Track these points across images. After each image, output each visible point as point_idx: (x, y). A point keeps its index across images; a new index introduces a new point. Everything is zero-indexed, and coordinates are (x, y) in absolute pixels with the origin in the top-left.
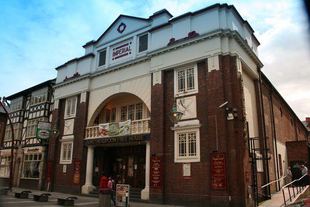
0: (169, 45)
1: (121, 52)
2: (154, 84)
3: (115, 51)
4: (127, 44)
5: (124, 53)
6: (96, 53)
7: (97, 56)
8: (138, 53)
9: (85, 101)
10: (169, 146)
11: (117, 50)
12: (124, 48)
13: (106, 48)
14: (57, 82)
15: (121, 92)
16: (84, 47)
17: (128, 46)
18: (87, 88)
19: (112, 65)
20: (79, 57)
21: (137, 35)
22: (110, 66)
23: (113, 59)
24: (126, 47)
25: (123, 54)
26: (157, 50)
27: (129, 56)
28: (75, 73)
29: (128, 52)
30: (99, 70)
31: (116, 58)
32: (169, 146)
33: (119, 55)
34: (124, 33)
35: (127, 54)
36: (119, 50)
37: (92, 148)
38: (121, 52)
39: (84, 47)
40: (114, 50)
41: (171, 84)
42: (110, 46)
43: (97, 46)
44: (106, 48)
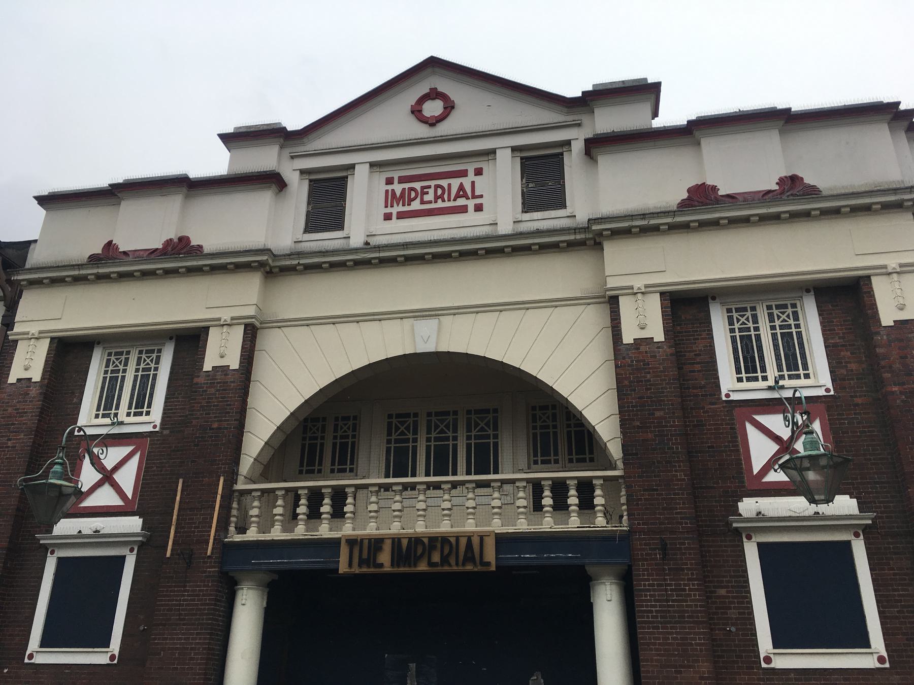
0: (685, 205)
1: (430, 197)
2: (628, 338)
3: (398, 188)
4: (464, 173)
5: (447, 204)
6: (290, 172)
7: (299, 190)
8: (300, 236)
9: (234, 363)
10: (723, 592)
11: (407, 186)
12: (444, 183)
13: (352, 167)
14: (36, 257)
15: (443, 348)
16: (226, 138)
17: (466, 182)
18: (251, 311)
19: (383, 240)
20: (195, 173)
21: (514, 149)
22: (374, 241)
23: (388, 217)
24: (455, 183)
25: (440, 204)
26: (643, 216)
27: (471, 217)
28: (172, 234)
29: (471, 204)
30: (523, 227)
31: (401, 216)
32: (723, 592)
33: (416, 205)
34: (443, 129)
35: (463, 209)
36: (417, 185)
37: (260, 585)
38: (426, 198)
39: (226, 138)
40: (389, 181)
41: (700, 346)
42: (372, 165)
43: (301, 149)
44: (352, 167)
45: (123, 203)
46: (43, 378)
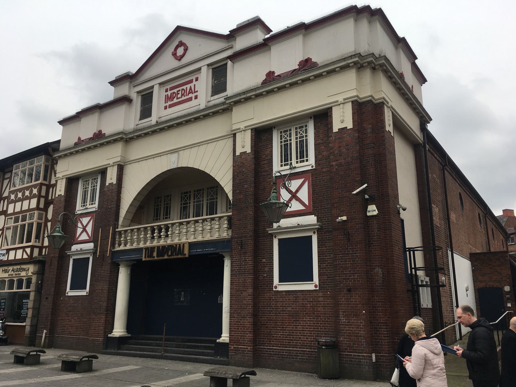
2: (238, 154)
3: (169, 93)
4: (191, 81)
7: (137, 101)
9: (114, 181)
10: (264, 260)
12: (184, 87)
13: (152, 87)
14: (62, 146)
15: (180, 166)
16: (112, 83)
17: (192, 85)
18: (119, 159)
19: (164, 119)
20: (102, 101)
21: (208, 65)
23: (166, 108)
24: (188, 86)
25: (183, 98)
26: (244, 93)
27: (194, 102)
30: (140, 126)
31: (171, 106)
32: (264, 260)
33: (175, 100)
34: (185, 60)
35: (190, 99)
36: (175, 91)
37: (127, 266)
38: (179, 96)
39: (112, 83)
40: (167, 91)
42: (160, 84)
44: (152, 87)
45: (82, 119)
46: (65, 194)
